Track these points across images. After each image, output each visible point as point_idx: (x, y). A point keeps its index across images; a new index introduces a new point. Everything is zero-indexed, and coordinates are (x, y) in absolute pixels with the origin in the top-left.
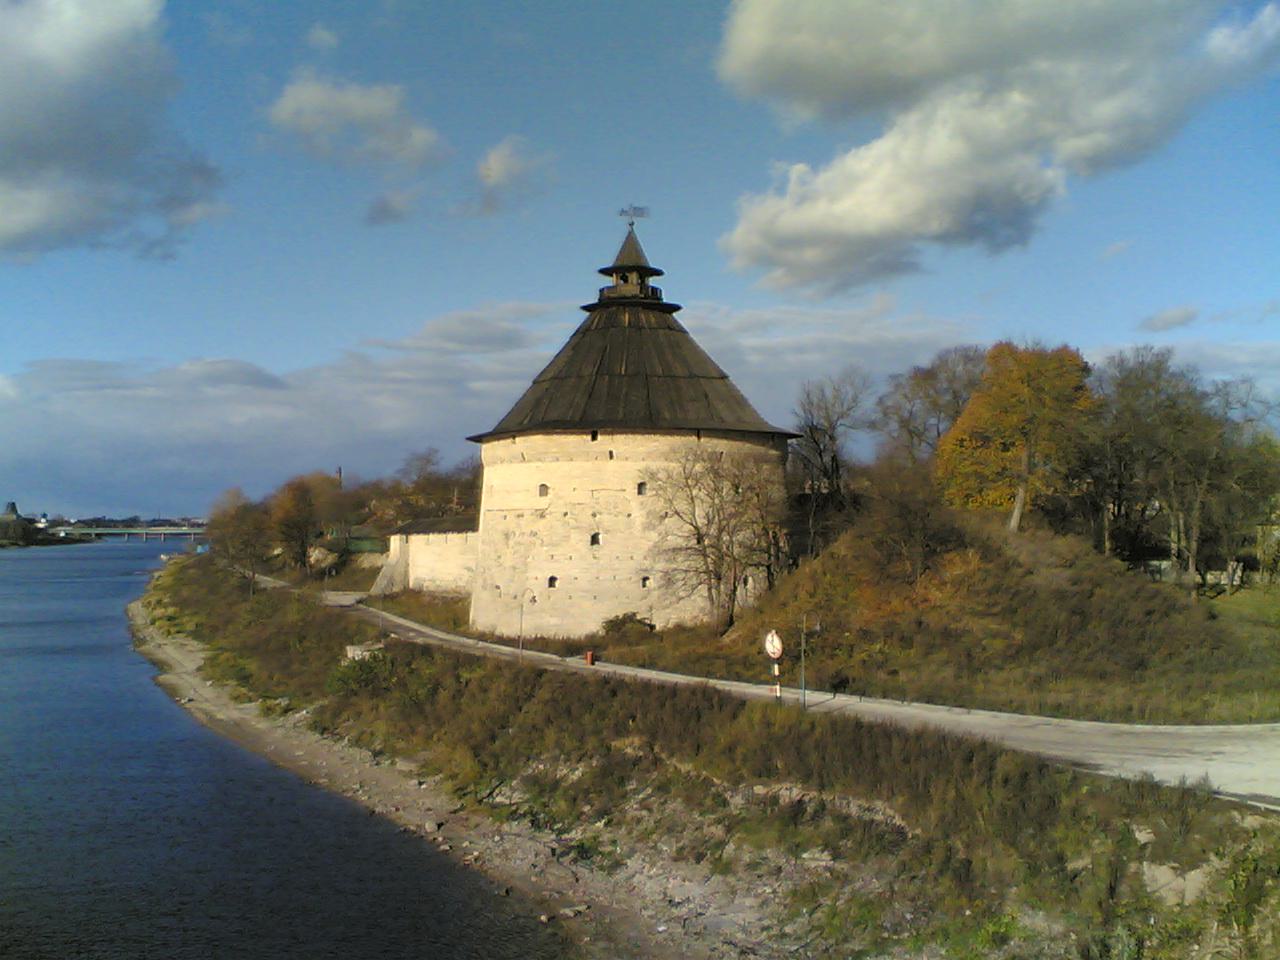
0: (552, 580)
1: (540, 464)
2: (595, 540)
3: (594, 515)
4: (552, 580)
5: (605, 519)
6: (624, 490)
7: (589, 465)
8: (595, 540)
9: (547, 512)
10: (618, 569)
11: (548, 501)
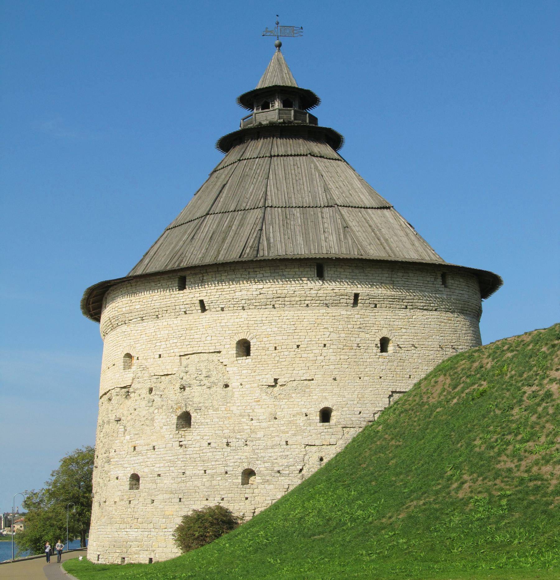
0: (135, 478)
1: (124, 327)
2: (185, 420)
3: (183, 388)
4: (135, 478)
5: (196, 395)
6: (219, 352)
7: (177, 321)
8: (185, 420)
9: (131, 390)
10: (209, 460)
11: (132, 375)
